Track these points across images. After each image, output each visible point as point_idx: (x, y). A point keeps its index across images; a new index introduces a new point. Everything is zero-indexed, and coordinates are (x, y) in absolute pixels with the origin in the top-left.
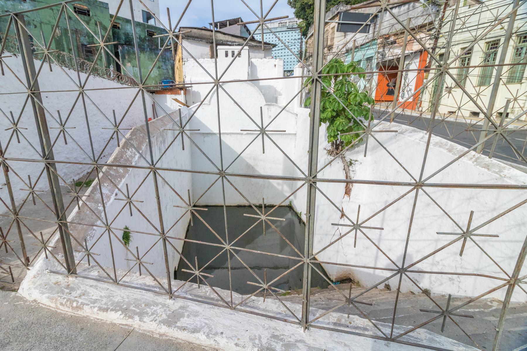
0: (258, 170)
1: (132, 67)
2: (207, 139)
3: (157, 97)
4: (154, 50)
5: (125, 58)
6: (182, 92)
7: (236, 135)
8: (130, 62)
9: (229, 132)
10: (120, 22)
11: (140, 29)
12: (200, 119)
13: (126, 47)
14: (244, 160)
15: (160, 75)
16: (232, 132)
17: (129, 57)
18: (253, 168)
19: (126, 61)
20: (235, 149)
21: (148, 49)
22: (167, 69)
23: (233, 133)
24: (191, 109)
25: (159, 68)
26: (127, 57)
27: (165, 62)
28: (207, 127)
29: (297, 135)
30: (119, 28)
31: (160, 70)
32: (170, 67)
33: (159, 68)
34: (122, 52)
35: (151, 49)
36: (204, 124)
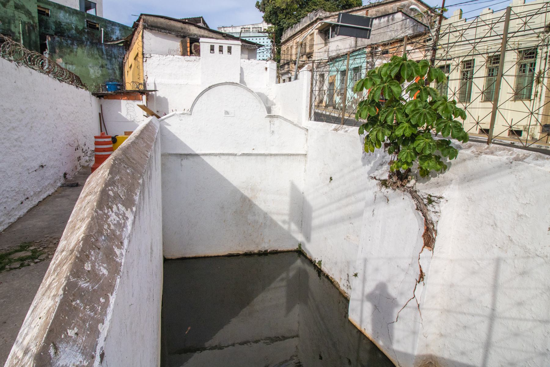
0: (257, 203)
2: (186, 162)
3: (107, 103)
4: (96, 44)
5: (55, 52)
6: (144, 97)
7: (227, 157)
8: (61, 57)
9: (218, 152)
10: (49, 7)
11: (77, 18)
12: (176, 135)
13: (57, 39)
14: (238, 190)
15: (103, 75)
16: (222, 152)
17: (61, 51)
18: (249, 200)
19: (56, 56)
20: (225, 176)
21: (88, 43)
22: (113, 69)
23: (223, 154)
24: (163, 120)
25: (102, 66)
26: (57, 51)
27: (110, 60)
28: (185, 145)
29: (308, 156)
30: (48, 15)
31: (104, 69)
32: (117, 67)
33: (102, 66)
34: (50, 43)
35: (92, 43)
36: (182, 142)
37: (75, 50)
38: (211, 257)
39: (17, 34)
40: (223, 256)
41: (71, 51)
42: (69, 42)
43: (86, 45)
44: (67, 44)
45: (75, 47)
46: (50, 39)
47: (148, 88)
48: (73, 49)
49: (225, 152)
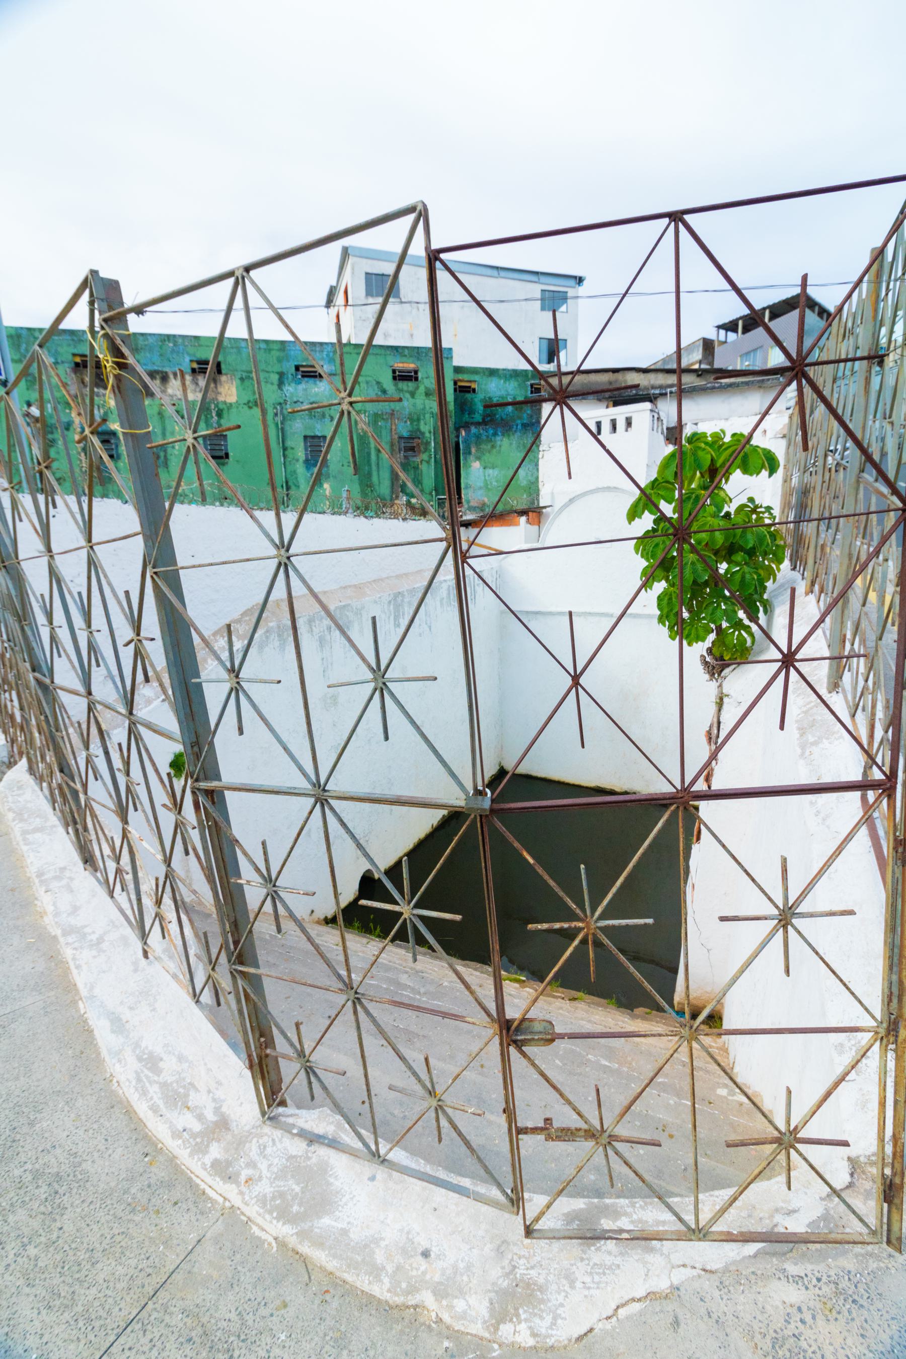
1: (481, 470)
5: (470, 453)
8: (478, 458)
10: (476, 378)
11: (516, 384)
17: (478, 449)
19: (472, 458)
21: (519, 427)
26: (473, 450)
30: (474, 390)
34: (465, 441)
37: (499, 443)
38: (568, 784)
39: (427, 435)
40: (587, 788)
41: (493, 447)
42: (491, 431)
43: (515, 431)
44: (488, 437)
45: (498, 438)
46: (463, 433)
47: (541, 505)
48: (495, 441)
49: (592, 611)
